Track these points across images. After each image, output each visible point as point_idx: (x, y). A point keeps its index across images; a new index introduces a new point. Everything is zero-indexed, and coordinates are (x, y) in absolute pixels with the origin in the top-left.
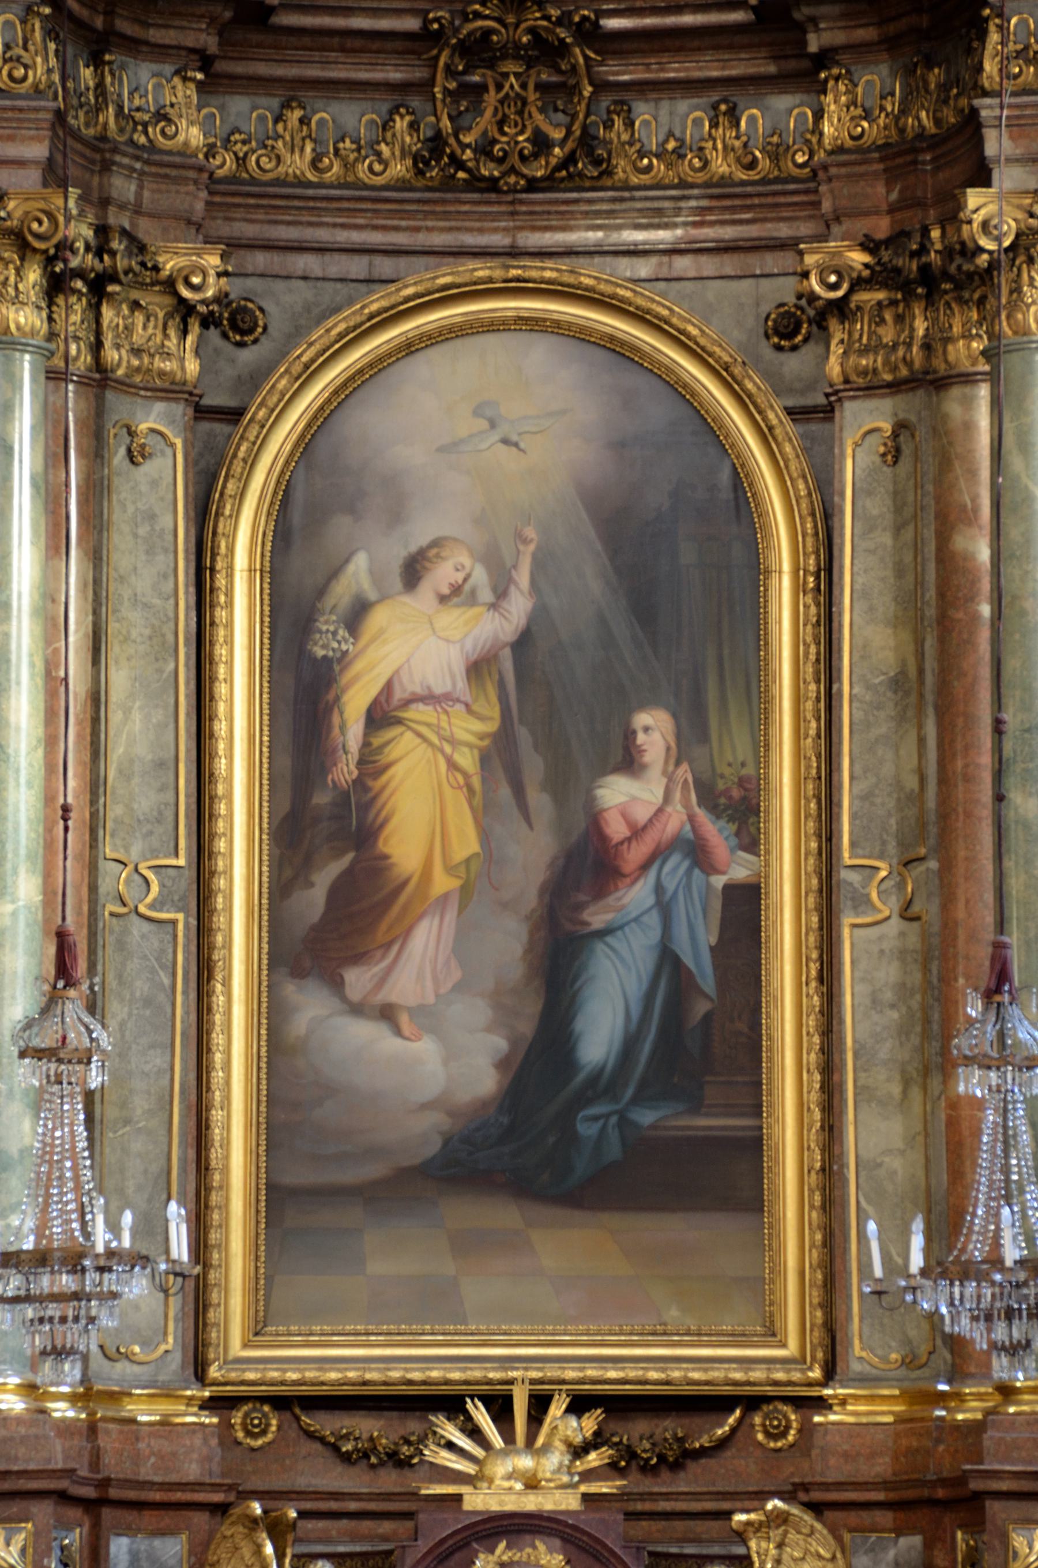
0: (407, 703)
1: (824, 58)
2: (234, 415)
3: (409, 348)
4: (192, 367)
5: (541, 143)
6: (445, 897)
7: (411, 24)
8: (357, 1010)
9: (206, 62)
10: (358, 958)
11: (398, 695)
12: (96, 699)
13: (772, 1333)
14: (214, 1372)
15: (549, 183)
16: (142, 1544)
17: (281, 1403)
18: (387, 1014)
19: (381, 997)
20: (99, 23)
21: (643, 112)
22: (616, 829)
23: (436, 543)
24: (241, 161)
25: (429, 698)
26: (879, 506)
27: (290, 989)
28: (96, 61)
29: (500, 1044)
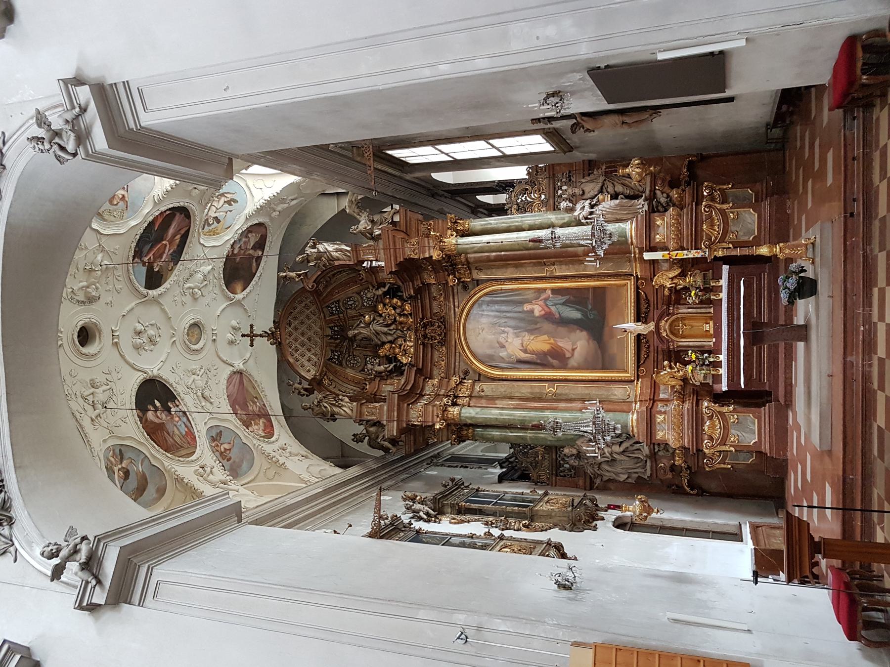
0: (523, 346)
1: (422, 283)
2: (480, 375)
3: (468, 347)
4: (470, 381)
5: (439, 326)
6: (554, 340)
7: (421, 346)
8: (573, 355)
9: (426, 378)
10: (564, 355)
11: (522, 348)
12: (521, 399)
13: (626, 285)
14: (633, 379)
15: (445, 325)
16: (661, 392)
17: (638, 367)
18: (573, 350)
19: (570, 351)
20: (418, 395)
21: (435, 311)
22: (543, 312)
23: (498, 342)
24: (443, 372)
25: (522, 344)
26: (489, 272)
27: (569, 366)
28: (424, 395)
29: (578, 331)
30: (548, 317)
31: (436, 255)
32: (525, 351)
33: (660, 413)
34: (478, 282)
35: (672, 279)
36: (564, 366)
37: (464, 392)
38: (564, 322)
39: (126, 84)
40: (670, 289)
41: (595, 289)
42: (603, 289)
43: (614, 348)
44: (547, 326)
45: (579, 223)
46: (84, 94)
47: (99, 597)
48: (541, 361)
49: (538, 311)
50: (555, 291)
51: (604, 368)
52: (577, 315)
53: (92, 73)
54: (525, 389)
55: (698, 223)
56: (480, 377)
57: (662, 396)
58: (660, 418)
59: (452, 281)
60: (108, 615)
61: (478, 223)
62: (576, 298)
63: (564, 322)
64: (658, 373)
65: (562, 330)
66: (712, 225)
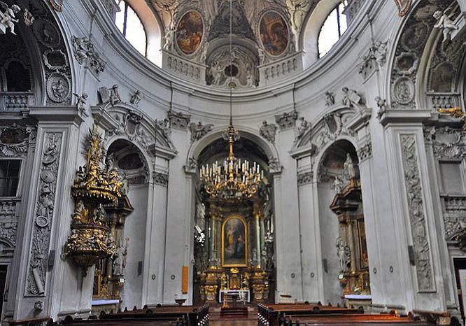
30: (238, 242)
31: (254, 213)
34: (247, 222)
37: (218, 219)
38: (237, 246)
41: (244, 256)
42: (244, 258)
43: (229, 261)
44: (235, 242)
45: (261, 252)
46: (280, 170)
47: (187, 170)
48: (226, 240)
49: (239, 239)
51: (225, 258)
52: (238, 250)
54: (219, 237)
55: (260, 284)
56: (222, 223)
59: (248, 215)
60: (183, 170)
61: (262, 223)
62: (243, 250)
63: (237, 246)
65: (234, 246)
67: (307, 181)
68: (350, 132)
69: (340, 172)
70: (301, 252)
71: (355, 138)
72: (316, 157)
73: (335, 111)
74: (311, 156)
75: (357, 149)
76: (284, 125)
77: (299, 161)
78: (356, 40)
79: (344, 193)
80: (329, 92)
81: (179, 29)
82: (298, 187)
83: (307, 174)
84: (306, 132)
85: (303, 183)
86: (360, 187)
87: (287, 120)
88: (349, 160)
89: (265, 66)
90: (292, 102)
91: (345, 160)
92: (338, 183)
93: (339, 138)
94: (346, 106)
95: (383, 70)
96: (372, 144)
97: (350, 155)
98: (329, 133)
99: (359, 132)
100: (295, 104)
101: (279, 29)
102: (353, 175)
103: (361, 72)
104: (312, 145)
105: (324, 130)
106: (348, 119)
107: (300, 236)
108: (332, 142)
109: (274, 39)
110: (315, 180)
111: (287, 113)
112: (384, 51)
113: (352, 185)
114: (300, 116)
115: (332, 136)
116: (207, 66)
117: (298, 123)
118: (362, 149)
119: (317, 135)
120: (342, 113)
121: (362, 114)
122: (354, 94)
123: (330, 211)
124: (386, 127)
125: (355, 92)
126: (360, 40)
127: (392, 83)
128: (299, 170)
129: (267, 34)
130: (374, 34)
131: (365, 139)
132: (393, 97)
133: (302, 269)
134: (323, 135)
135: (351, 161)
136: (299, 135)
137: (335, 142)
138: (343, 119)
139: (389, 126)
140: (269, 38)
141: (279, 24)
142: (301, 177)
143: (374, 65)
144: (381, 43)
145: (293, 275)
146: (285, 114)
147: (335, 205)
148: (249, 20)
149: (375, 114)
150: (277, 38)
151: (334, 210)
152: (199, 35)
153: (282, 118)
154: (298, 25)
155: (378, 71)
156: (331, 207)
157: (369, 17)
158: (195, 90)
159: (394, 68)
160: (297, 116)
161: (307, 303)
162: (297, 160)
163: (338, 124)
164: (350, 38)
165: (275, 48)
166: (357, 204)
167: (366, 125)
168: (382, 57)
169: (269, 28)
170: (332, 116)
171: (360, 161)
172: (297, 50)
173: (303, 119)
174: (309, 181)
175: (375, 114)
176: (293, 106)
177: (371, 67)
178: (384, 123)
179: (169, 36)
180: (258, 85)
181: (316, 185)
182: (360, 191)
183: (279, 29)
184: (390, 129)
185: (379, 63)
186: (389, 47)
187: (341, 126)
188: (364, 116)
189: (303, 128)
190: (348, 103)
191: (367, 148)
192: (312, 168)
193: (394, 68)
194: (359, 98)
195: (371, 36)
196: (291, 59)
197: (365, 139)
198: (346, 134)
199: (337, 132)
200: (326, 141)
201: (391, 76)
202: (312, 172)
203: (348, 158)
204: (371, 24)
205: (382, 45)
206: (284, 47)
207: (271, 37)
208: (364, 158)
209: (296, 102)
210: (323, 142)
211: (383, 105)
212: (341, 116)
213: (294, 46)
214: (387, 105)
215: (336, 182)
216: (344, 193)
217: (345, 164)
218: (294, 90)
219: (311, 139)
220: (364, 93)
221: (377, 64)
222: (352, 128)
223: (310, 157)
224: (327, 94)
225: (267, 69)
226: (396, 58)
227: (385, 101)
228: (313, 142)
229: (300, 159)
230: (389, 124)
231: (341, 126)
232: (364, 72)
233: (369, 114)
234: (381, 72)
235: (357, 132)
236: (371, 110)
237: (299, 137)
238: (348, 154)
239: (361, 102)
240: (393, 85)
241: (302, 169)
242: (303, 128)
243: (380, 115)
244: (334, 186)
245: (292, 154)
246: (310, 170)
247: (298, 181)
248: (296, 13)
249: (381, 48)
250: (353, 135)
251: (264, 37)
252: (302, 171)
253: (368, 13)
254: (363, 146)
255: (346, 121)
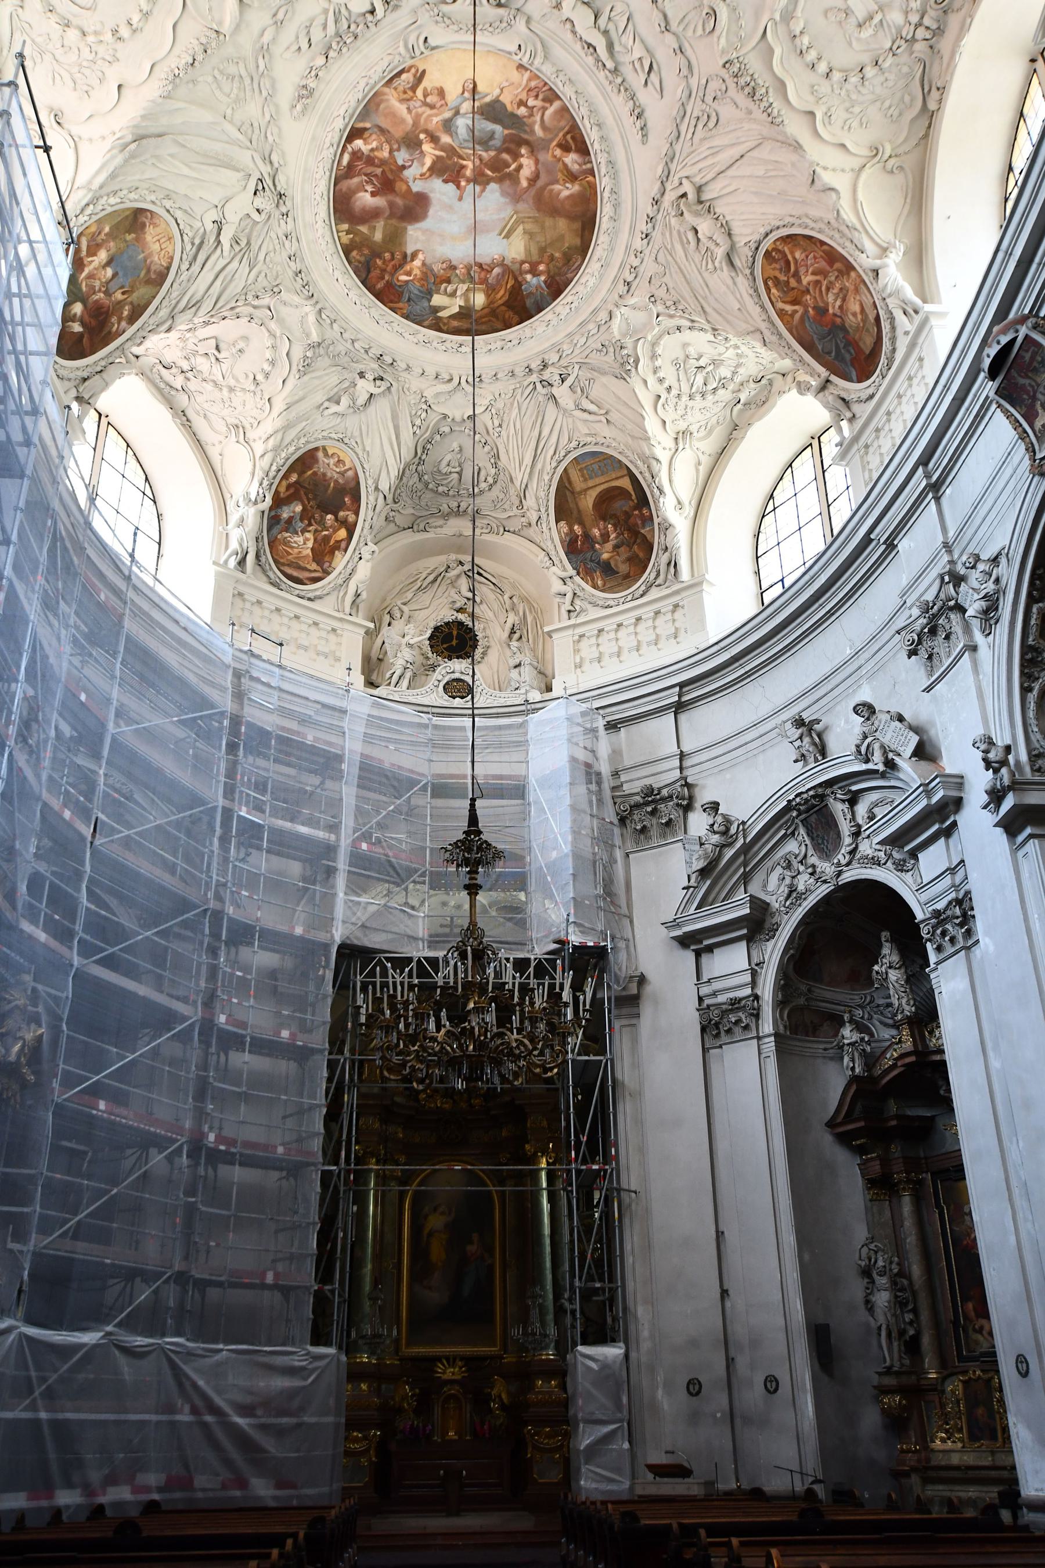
13: (495, 1346)
32: (430, 1234)
33: (369, 1387)
35: (500, 1396)
36: (413, 1277)
39: (638, 1016)
40: (490, 1394)
48: (419, 1251)
49: (472, 1249)
50: (491, 1268)
53: (648, 989)
57: (383, 1386)
58: (364, 1387)
64: (407, 1383)
66: (549, 1436)
67: (737, 1030)
68: (889, 856)
69: (858, 1001)
70: (724, 1293)
71: (908, 877)
72: (770, 944)
73: (830, 783)
74: (750, 939)
75: (919, 915)
76: (644, 829)
77: (705, 958)
78: (891, 545)
79: (877, 1071)
80: (804, 715)
81: (278, 502)
82: (705, 1050)
83: (735, 1004)
84: (729, 853)
85: (724, 1038)
86: (942, 1052)
87: (653, 813)
88: (889, 954)
89: (574, 626)
90: (675, 750)
91: (875, 957)
92: (856, 1037)
93: (848, 876)
94: (870, 766)
95: (992, 647)
96: (974, 896)
97: (893, 940)
98: (813, 860)
99: (921, 856)
100: (682, 756)
101: (620, 506)
102: (908, 1010)
103: (913, 653)
104: (754, 901)
105: (792, 846)
106: (879, 812)
107: (719, 1235)
108: (823, 890)
109: (605, 538)
110: (767, 1026)
111: (655, 786)
112: (991, 587)
113: (908, 1045)
114: (704, 796)
115: (827, 868)
116: (372, 625)
117: (698, 823)
118: (937, 914)
119: (769, 863)
120: (854, 788)
121: (929, 794)
122: (897, 723)
123: (828, 1139)
124: (1020, 838)
125: (901, 719)
126: (904, 545)
127: (1025, 690)
128: (705, 990)
129: (581, 524)
130: (951, 534)
131: (947, 881)
132: (1036, 737)
133: (730, 1362)
134: (789, 866)
135: (895, 958)
136: (701, 864)
137: (839, 888)
138: (861, 809)
139: (1031, 836)
140: (587, 536)
141: (621, 492)
142: (715, 1015)
143: (957, 628)
144: (977, 558)
145: (694, 1388)
146: (649, 791)
147: (849, 1117)
148: (520, 476)
149: (976, 794)
150: (612, 536)
151: (844, 1139)
152: (343, 523)
153: (637, 806)
154: (685, 498)
155: (974, 648)
156: (831, 1124)
157: (928, 476)
158: (324, 706)
159: (1031, 641)
160: (691, 798)
161: (757, 1494)
162: (698, 954)
163: (845, 828)
164: (867, 541)
165: (607, 569)
166: (927, 1113)
167: (948, 832)
168: (983, 604)
169: (588, 502)
170: (822, 797)
171: (933, 957)
172: (685, 574)
173: (714, 807)
174: (747, 1028)
175: (976, 794)
176: (677, 763)
177: (947, 637)
178: (1011, 825)
179: (241, 522)
180: (549, 689)
181: (770, 1044)
182: (941, 1068)
183: (620, 506)
184: (1033, 846)
185: (975, 624)
186: (1008, 573)
187: (857, 834)
188: (935, 799)
189: (715, 838)
190: (877, 757)
191: (958, 911)
192: (754, 983)
193: (1031, 641)
194: (914, 740)
195: (941, 539)
196: (666, 605)
197: (947, 881)
198: (876, 862)
199: (842, 857)
200: (801, 887)
201: (1022, 666)
202: (757, 997)
203: (886, 950)
204: (937, 499)
205: (981, 566)
206: (640, 564)
207: (596, 532)
208: (949, 950)
209: (686, 749)
210: (792, 889)
211: (1004, 763)
212: (853, 800)
213: (673, 564)
214: (1018, 763)
215: (848, 1034)
216: (877, 1071)
217: (876, 968)
218: (679, 707)
219: (746, 878)
220: (934, 724)
221: (967, 629)
222: (896, 840)
223: (743, 945)
224: (799, 723)
225: (582, 636)
226: (1035, 610)
227: (1008, 749)
228: (754, 888)
229: (710, 949)
230: (1028, 830)
231: (857, 834)
232: (923, 654)
233: (954, 793)
234: (984, 652)
235: (914, 854)
236: (959, 782)
237: (703, 873)
238: (885, 935)
239: (924, 752)
240: (1032, 697)
241: (717, 985)
242: (715, 838)
243: (996, 796)
244: (841, 1048)
245: (678, 933)
246: (748, 991)
247: (703, 1030)
248: (681, 456)
249: (974, 577)
250: (900, 867)
251: (571, 530)
252: (714, 994)
253: (924, 460)
254: (940, 905)
255: (872, 817)
